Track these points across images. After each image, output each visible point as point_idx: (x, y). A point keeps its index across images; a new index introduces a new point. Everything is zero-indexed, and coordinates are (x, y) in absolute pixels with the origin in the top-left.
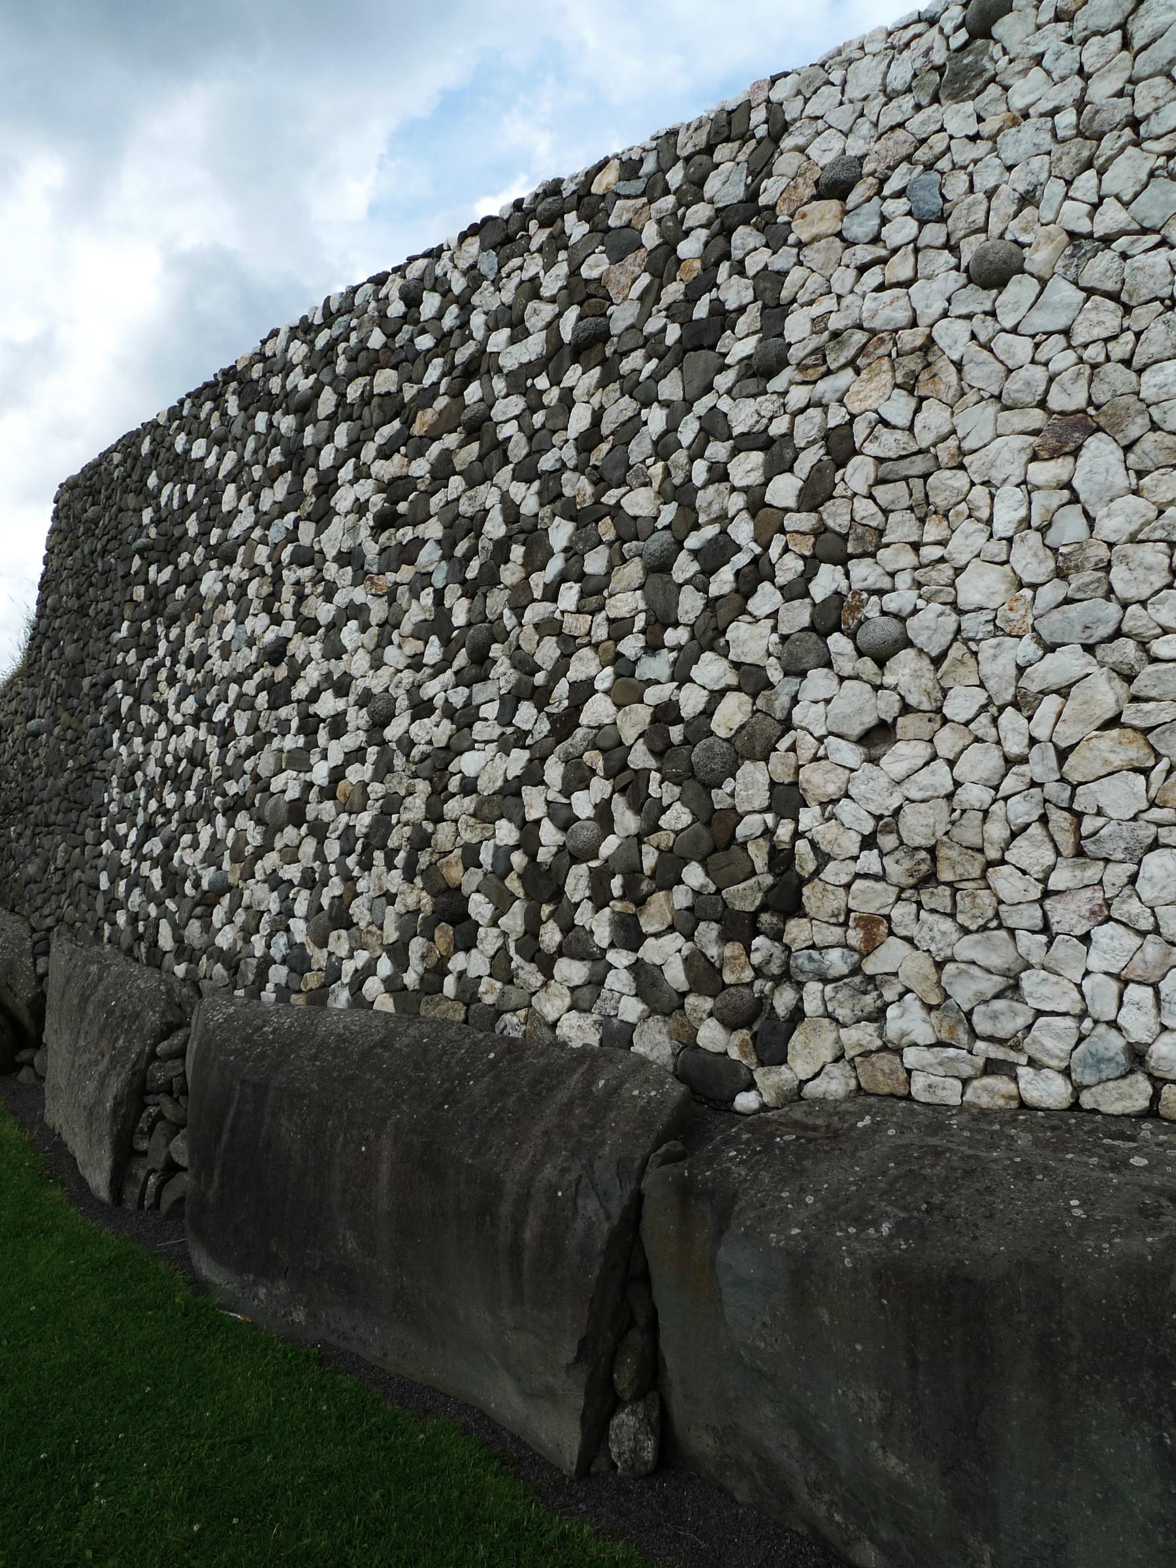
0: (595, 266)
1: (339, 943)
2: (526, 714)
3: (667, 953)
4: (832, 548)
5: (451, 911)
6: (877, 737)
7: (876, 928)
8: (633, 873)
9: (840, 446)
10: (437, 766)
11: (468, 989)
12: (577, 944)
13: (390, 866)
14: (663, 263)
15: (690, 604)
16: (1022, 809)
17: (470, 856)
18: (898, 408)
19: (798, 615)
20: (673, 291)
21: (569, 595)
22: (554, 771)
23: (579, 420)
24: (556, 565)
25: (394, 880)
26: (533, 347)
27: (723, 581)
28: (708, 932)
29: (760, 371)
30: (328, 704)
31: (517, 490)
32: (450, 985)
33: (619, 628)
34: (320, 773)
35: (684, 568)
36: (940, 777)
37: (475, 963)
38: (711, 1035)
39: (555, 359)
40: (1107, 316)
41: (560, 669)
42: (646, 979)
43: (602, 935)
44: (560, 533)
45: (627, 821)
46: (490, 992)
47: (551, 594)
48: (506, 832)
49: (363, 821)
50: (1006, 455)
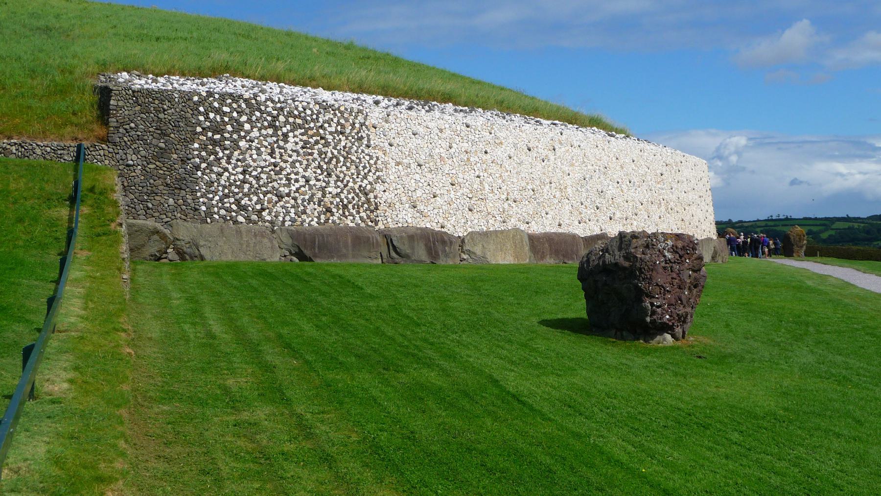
0: (342, 121)
1: (304, 217)
2: (339, 183)
3: (363, 214)
4: (377, 170)
5: (328, 210)
6: (385, 191)
8: (358, 205)
9: (378, 158)
10: (323, 189)
11: (334, 222)
12: (351, 214)
15: (362, 173)
17: (332, 203)
19: (375, 177)
20: (355, 131)
21: (344, 168)
22: (345, 192)
23: (343, 144)
25: (316, 206)
26: (333, 129)
27: (366, 171)
28: (368, 212)
29: (368, 146)
30: (293, 176)
33: (353, 174)
34: (294, 188)
35: (361, 168)
38: (370, 223)
39: (336, 131)
40: (400, 153)
44: (342, 159)
45: (356, 199)
46: (338, 221)
48: (338, 200)
49: (307, 197)
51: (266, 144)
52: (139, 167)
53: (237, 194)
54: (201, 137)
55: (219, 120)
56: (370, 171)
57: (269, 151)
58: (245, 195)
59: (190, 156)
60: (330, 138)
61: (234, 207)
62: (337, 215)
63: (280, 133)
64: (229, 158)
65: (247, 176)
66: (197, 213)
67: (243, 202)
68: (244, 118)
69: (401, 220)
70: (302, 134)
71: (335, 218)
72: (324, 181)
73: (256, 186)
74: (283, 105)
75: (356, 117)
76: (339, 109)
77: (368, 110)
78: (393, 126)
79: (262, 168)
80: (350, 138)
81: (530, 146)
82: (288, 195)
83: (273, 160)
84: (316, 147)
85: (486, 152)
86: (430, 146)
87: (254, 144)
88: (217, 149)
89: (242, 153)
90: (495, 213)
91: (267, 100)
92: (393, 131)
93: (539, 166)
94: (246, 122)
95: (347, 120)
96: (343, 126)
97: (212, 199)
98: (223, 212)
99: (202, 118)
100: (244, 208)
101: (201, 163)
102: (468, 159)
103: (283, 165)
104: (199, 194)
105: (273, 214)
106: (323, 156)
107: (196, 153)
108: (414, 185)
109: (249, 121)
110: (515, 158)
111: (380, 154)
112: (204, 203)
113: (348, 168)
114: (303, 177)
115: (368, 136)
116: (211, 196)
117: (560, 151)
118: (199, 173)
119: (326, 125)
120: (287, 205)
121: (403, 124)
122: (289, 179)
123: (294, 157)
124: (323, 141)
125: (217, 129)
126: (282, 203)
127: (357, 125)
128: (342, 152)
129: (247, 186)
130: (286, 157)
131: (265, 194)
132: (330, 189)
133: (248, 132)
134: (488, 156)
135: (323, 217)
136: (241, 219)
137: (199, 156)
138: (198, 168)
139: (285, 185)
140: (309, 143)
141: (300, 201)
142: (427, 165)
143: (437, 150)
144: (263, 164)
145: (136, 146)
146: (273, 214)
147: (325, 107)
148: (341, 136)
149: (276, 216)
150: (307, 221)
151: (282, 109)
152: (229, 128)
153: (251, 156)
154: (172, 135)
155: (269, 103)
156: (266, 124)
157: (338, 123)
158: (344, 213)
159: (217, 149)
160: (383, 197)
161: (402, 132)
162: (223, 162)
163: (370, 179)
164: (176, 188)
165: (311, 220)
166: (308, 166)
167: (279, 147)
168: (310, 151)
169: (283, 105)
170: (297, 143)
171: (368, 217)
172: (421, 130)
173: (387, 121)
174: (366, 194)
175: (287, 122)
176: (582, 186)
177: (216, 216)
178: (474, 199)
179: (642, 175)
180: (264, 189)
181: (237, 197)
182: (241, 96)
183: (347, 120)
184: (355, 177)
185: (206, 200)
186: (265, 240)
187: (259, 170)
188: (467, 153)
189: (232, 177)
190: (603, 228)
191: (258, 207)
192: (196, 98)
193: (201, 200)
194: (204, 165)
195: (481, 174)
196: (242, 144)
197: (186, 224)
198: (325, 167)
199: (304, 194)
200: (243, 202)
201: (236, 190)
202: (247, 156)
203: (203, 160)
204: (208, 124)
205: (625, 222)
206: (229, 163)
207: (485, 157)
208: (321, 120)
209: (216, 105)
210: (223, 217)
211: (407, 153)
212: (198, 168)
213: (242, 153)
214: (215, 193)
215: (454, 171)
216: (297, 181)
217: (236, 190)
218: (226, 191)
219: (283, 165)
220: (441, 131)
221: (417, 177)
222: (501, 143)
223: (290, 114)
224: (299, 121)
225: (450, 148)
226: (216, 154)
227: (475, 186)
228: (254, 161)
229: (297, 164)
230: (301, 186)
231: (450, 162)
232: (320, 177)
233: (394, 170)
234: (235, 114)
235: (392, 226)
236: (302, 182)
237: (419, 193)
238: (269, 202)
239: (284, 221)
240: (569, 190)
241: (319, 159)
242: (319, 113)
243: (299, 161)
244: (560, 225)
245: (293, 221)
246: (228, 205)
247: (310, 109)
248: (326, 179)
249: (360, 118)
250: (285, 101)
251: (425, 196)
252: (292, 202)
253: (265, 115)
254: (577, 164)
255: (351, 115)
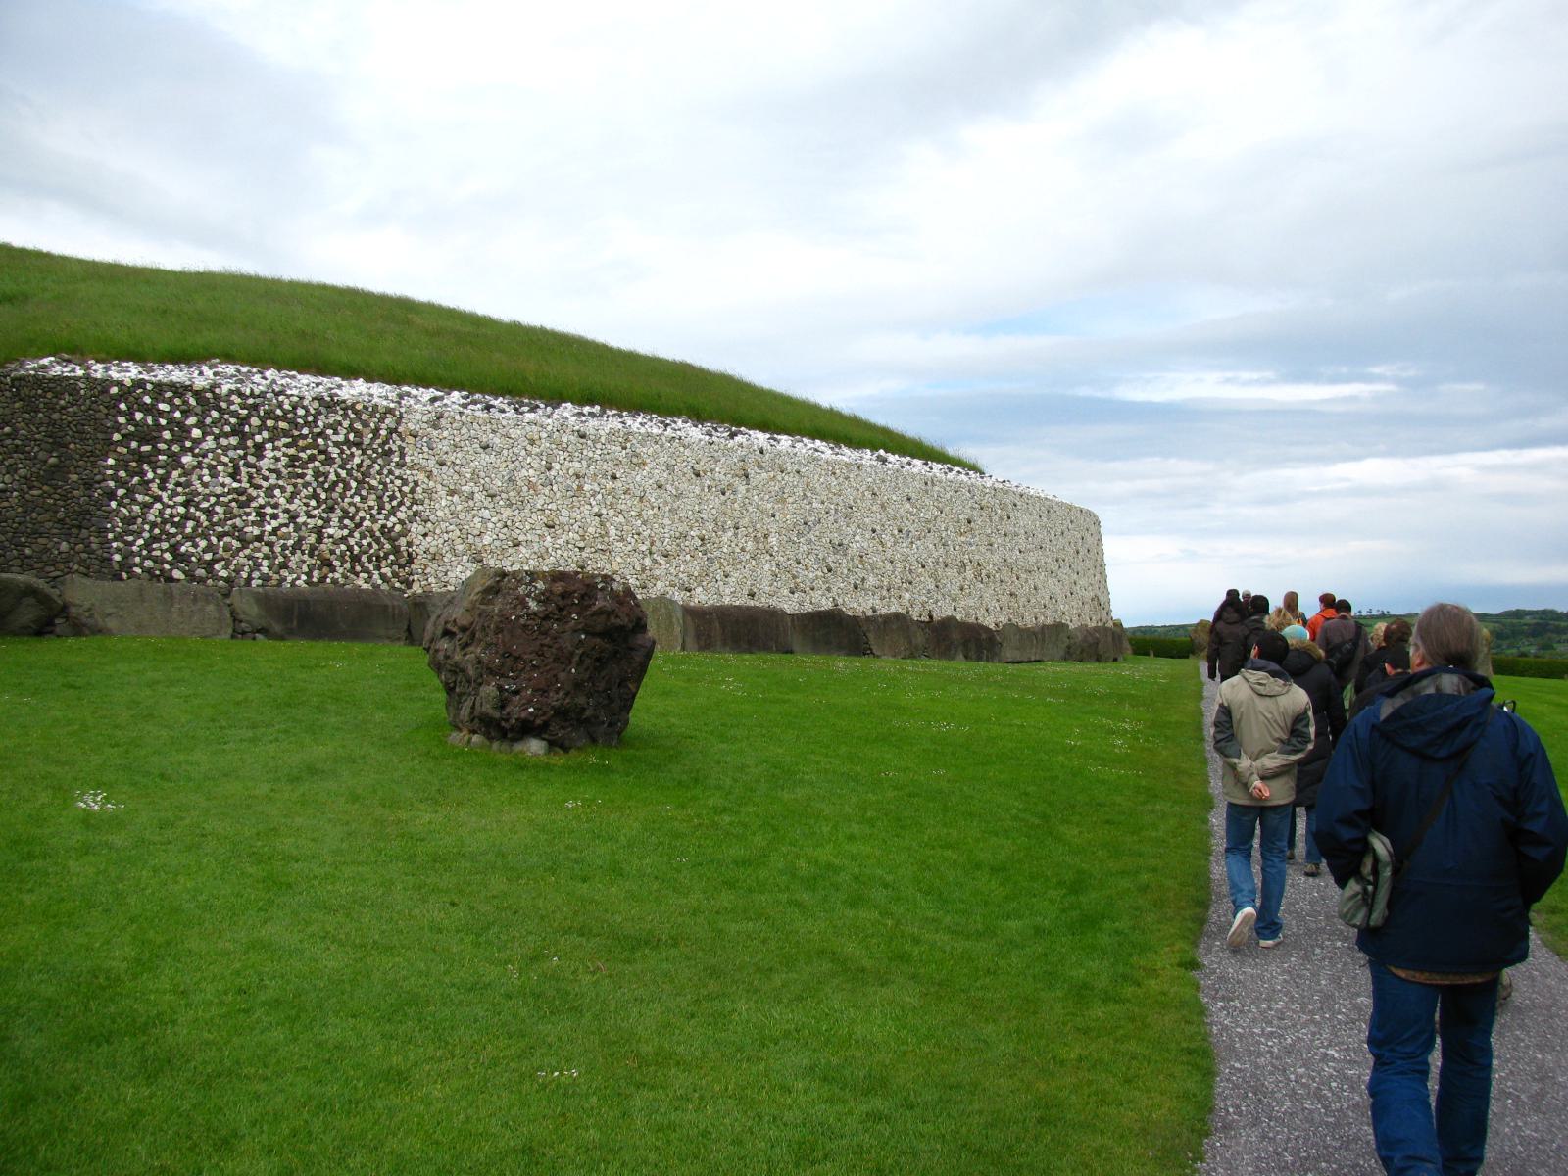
0: (358, 426)
1: (284, 573)
2: (347, 522)
3: (387, 571)
4: (415, 502)
6: (425, 535)
7: (426, 565)
8: (378, 557)
9: (416, 484)
11: (335, 582)
13: (303, 553)
14: (376, 432)
15: (388, 506)
16: (447, 548)
17: (332, 552)
18: (426, 480)
19: (410, 513)
20: (379, 441)
21: (357, 499)
23: (357, 460)
24: (353, 491)
25: (306, 557)
26: (341, 438)
27: (395, 503)
28: (396, 568)
29: (401, 465)
30: (269, 510)
31: (339, 470)
32: (329, 580)
33: (371, 508)
34: (268, 528)
35: (386, 499)
36: (435, 543)
37: (337, 576)
38: (397, 585)
39: (347, 441)
40: (456, 477)
41: (355, 514)
42: (383, 577)
43: (372, 568)
44: (354, 484)
45: (376, 546)
46: (341, 581)
47: (352, 497)
48: (343, 547)
49: (290, 542)
50: (443, 493)
51: (226, 459)
52: (15, 494)
53: (174, 535)
54: (119, 449)
55: (150, 422)
56: (401, 503)
57: (230, 471)
58: (188, 538)
59: (98, 478)
60: (334, 451)
61: (168, 556)
62: (341, 570)
63: (250, 443)
64: (164, 480)
65: (192, 510)
66: (105, 564)
67: (183, 549)
68: (192, 420)
69: (453, 581)
70: (287, 446)
71: (337, 576)
72: (321, 518)
73: (206, 524)
74: (258, 400)
75: (382, 420)
76: (353, 405)
77: (403, 410)
78: (445, 434)
79: (218, 496)
80: (370, 452)
81: (696, 466)
82: (259, 538)
83: (235, 485)
84: (310, 465)
85: (614, 477)
86: (511, 466)
87: (206, 460)
88: (146, 467)
89: (185, 474)
90: (627, 572)
91: (231, 392)
92: (445, 442)
93: (717, 501)
94: (196, 426)
95: (365, 424)
96: (358, 433)
97: (132, 543)
98: (148, 563)
99: (122, 420)
100: (184, 558)
101: (117, 488)
102: (580, 488)
103: (254, 493)
104: (110, 536)
105: (232, 568)
106: (322, 479)
107: (110, 472)
108: (479, 526)
109: (200, 425)
110: (669, 487)
111: (421, 477)
112: (118, 550)
113: (364, 499)
114: (287, 511)
115: (401, 449)
116: (131, 538)
117: (759, 478)
118: (113, 504)
119: (330, 432)
120: (257, 554)
121: (464, 430)
122: (261, 515)
123: (273, 480)
124: (323, 457)
125: (148, 436)
126: (247, 551)
127: (383, 433)
128: (355, 473)
129: (190, 524)
130: (259, 481)
131: (220, 537)
132: (331, 531)
133: (197, 442)
134: (618, 484)
135: (316, 574)
136: (177, 574)
137: (115, 478)
138: (112, 495)
139: (253, 523)
140: (300, 458)
141: (278, 549)
142: (504, 495)
143: (524, 473)
144: (218, 490)
145: (11, 461)
146: (232, 568)
147: (330, 404)
148: (354, 449)
149: (238, 572)
150: (289, 579)
151: (255, 407)
152: (167, 435)
153: (200, 478)
154: (72, 446)
155: (234, 397)
156: (227, 429)
157: (351, 429)
158: (353, 568)
159: (146, 467)
160: (421, 545)
161: (462, 444)
162: (154, 487)
163: (401, 515)
164: (73, 526)
165: (298, 577)
166: (293, 495)
167: (248, 465)
168: (300, 471)
169: (258, 400)
170: (278, 459)
171: (395, 575)
172: (497, 440)
173: (436, 427)
174: (392, 540)
175: (262, 427)
176: (799, 534)
177: (138, 570)
178: (588, 550)
179: (928, 522)
180: (220, 529)
181: (173, 541)
182: (188, 388)
183: (365, 424)
184: (374, 512)
185: (121, 545)
186: (211, 607)
187: (213, 499)
188: (578, 477)
189: (168, 511)
190: (840, 601)
191: (208, 556)
192: (114, 390)
193: (114, 545)
194: (121, 492)
195: (604, 511)
196: (187, 459)
197: (85, 581)
198: (323, 496)
199: (287, 537)
200: (183, 549)
201: (173, 530)
202: (194, 477)
203: (121, 483)
204: (132, 428)
205: (885, 593)
206: (163, 488)
207: (610, 485)
208: (320, 424)
209: (147, 400)
210: (149, 571)
211: (469, 476)
212: (112, 495)
213: (185, 474)
214: (139, 534)
215: (553, 506)
216: (275, 517)
217: (173, 530)
218: (157, 531)
219: (254, 493)
220: (532, 442)
221: (486, 513)
222: (644, 464)
223: (269, 414)
224: (283, 425)
225: (549, 469)
226: (143, 474)
227: (591, 530)
228: (205, 485)
229: (277, 492)
230: (282, 526)
231: (546, 491)
232: (316, 512)
233: (443, 504)
234: (178, 415)
235: (435, 588)
236: (283, 518)
237: (487, 539)
238: (227, 548)
239: (249, 579)
240: (773, 540)
241: (314, 484)
242: (318, 412)
243: (280, 487)
244: (752, 595)
245: (265, 578)
246: (158, 553)
247: (303, 407)
248: (325, 515)
249: (389, 421)
250: (262, 395)
251: (497, 543)
252: (266, 549)
253: (226, 416)
254: (790, 500)
255: (372, 415)
